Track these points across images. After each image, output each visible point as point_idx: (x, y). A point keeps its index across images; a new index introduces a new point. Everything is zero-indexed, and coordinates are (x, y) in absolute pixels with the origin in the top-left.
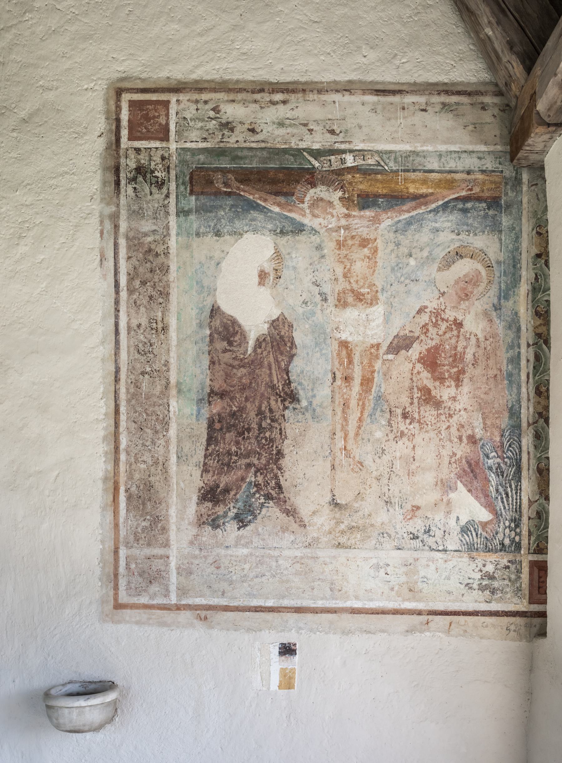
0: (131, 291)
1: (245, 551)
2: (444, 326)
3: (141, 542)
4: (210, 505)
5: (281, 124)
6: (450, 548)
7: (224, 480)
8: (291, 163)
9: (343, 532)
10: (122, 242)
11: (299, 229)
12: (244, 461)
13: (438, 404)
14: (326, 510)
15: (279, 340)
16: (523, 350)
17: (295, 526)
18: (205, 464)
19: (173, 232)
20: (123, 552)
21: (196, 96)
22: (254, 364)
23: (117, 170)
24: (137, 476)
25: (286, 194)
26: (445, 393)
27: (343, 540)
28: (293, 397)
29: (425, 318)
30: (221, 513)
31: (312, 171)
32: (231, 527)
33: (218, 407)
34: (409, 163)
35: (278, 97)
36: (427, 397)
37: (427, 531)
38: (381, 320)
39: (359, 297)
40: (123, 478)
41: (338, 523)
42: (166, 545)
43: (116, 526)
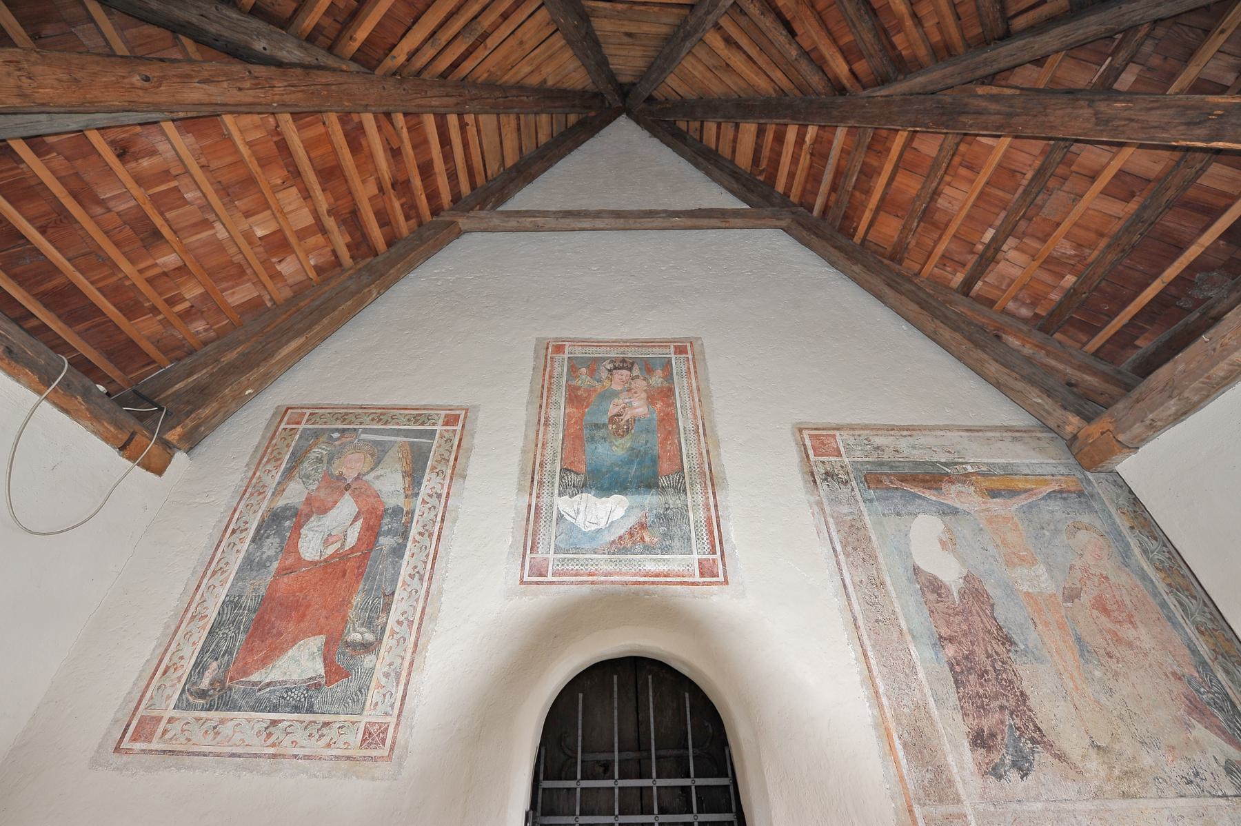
0: (847, 555)
1: (1039, 806)
2: (1096, 580)
3: (932, 798)
4: (983, 751)
5: (914, 448)
6: (1228, 793)
7: (987, 724)
8: (930, 470)
9: (1120, 778)
10: (830, 520)
11: (955, 512)
12: (994, 704)
13: (1130, 645)
14: (1093, 753)
15: (974, 591)
16: (1166, 597)
17: (1072, 774)
18: (962, 707)
19: (865, 513)
20: (917, 811)
21: (851, 432)
22: (964, 612)
23: (812, 474)
24: (905, 722)
25: (936, 489)
26: (1129, 633)
27: (1125, 788)
28: (1008, 640)
29: (1078, 574)
30: (997, 761)
31: (947, 474)
32: (1014, 775)
33: (951, 651)
34: (1009, 471)
35: (905, 433)
36: (1119, 641)
37: (1197, 774)
38: (1046, 575)
39: (1022, 559)
40: (892, 725)
41: (1111, 768)
42: (959, 801)
43: (902, 779)
